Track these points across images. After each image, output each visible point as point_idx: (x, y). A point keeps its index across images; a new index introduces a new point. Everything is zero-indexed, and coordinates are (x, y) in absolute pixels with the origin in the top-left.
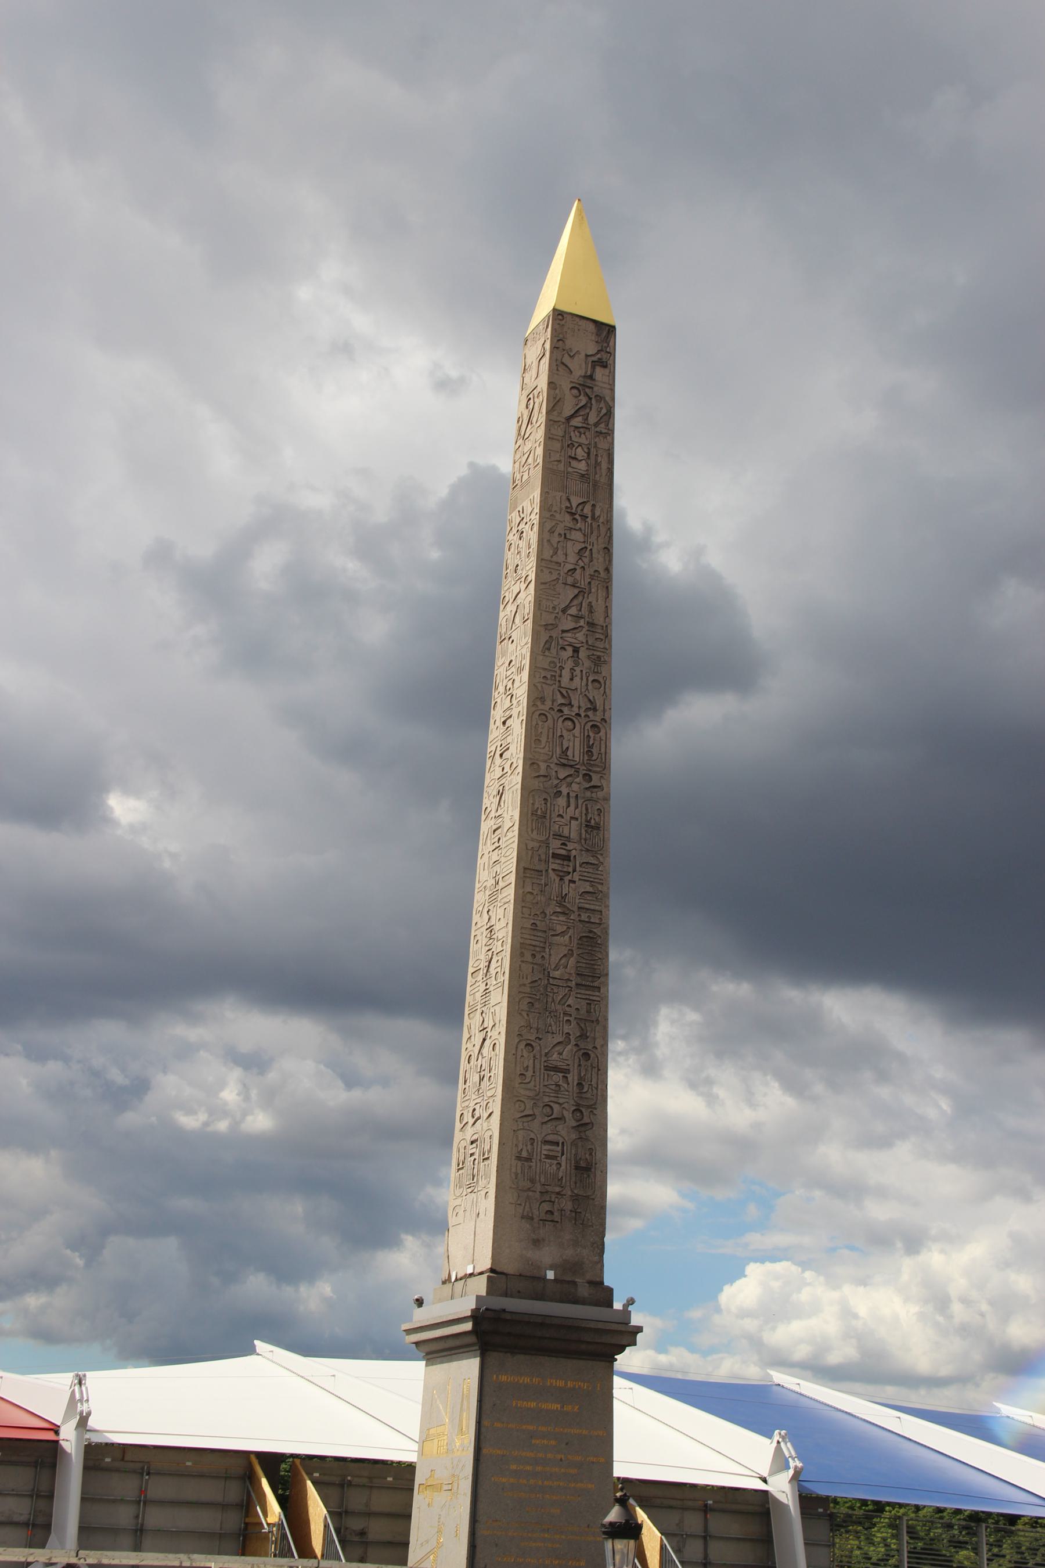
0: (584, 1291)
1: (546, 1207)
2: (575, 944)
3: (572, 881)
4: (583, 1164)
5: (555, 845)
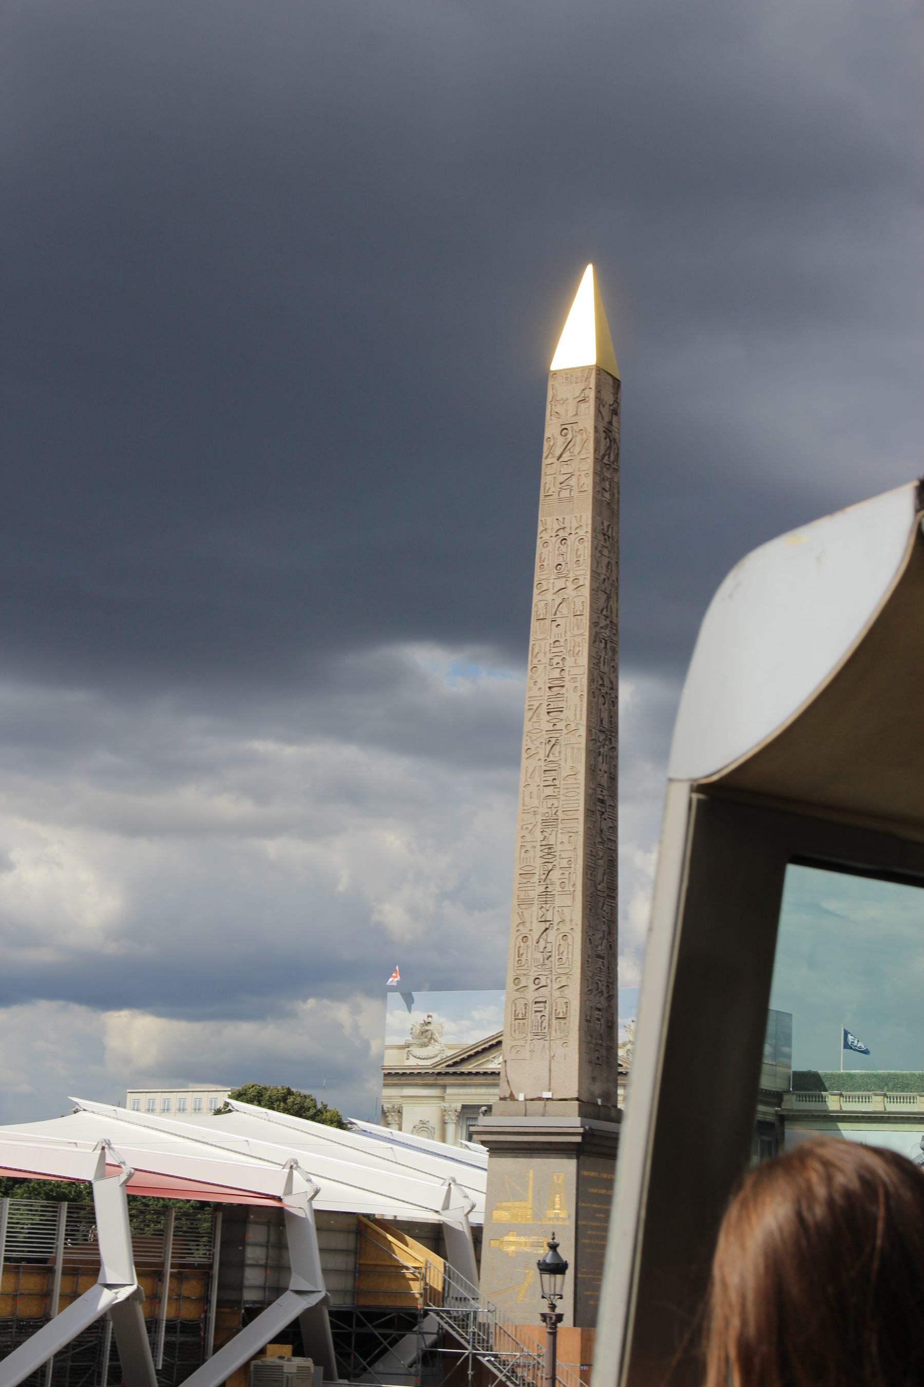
0: (613, 1113)
5: (599, 790)
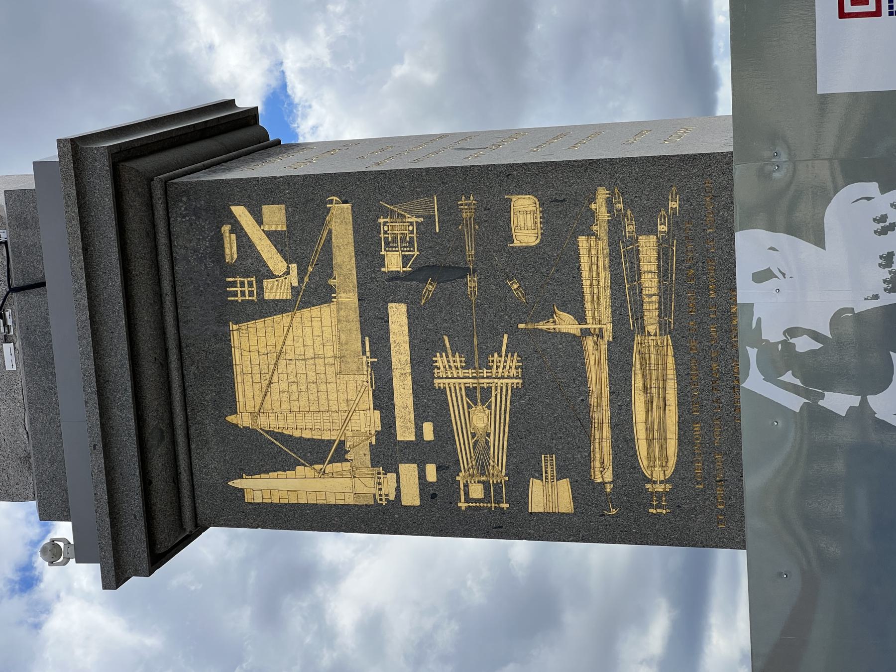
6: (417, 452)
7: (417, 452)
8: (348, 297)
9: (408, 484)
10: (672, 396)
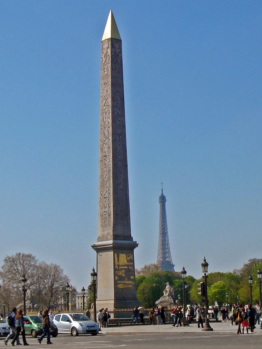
1: (105, 224)
2: (107, 172)
3: (106, 160)
4: (109, 214)
5: (104, 154)
6: (119, 268)
7: (119, 268)
8: (128, 264)
9: (117, 267)
10: (123, 287)
